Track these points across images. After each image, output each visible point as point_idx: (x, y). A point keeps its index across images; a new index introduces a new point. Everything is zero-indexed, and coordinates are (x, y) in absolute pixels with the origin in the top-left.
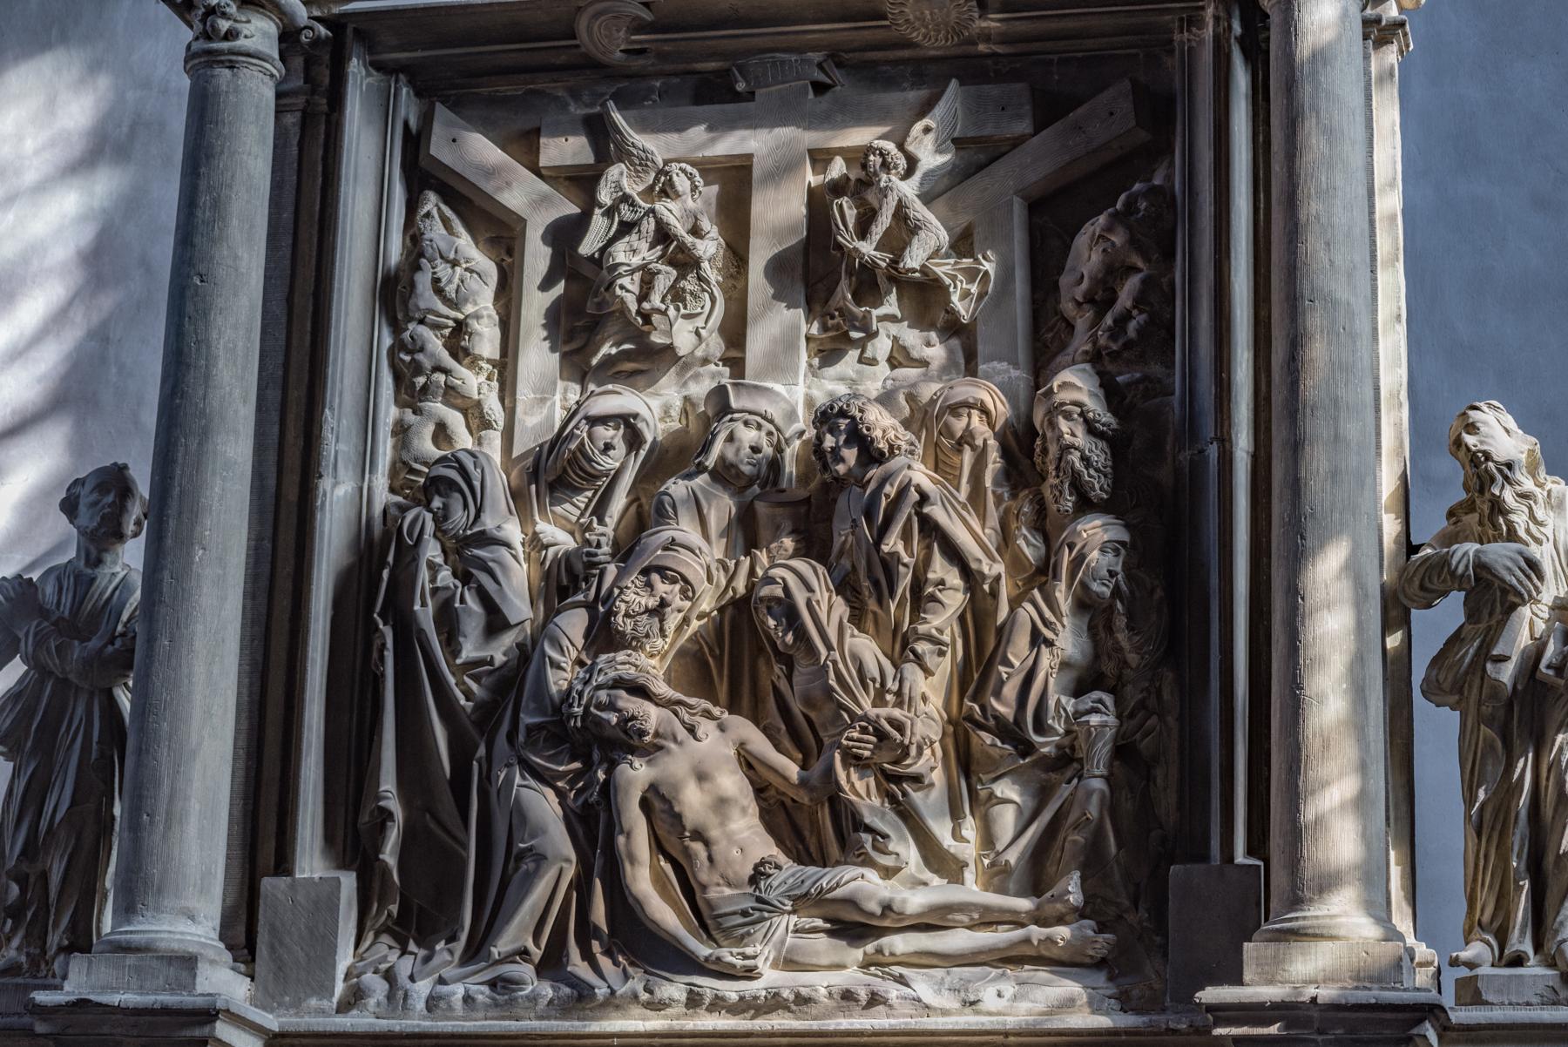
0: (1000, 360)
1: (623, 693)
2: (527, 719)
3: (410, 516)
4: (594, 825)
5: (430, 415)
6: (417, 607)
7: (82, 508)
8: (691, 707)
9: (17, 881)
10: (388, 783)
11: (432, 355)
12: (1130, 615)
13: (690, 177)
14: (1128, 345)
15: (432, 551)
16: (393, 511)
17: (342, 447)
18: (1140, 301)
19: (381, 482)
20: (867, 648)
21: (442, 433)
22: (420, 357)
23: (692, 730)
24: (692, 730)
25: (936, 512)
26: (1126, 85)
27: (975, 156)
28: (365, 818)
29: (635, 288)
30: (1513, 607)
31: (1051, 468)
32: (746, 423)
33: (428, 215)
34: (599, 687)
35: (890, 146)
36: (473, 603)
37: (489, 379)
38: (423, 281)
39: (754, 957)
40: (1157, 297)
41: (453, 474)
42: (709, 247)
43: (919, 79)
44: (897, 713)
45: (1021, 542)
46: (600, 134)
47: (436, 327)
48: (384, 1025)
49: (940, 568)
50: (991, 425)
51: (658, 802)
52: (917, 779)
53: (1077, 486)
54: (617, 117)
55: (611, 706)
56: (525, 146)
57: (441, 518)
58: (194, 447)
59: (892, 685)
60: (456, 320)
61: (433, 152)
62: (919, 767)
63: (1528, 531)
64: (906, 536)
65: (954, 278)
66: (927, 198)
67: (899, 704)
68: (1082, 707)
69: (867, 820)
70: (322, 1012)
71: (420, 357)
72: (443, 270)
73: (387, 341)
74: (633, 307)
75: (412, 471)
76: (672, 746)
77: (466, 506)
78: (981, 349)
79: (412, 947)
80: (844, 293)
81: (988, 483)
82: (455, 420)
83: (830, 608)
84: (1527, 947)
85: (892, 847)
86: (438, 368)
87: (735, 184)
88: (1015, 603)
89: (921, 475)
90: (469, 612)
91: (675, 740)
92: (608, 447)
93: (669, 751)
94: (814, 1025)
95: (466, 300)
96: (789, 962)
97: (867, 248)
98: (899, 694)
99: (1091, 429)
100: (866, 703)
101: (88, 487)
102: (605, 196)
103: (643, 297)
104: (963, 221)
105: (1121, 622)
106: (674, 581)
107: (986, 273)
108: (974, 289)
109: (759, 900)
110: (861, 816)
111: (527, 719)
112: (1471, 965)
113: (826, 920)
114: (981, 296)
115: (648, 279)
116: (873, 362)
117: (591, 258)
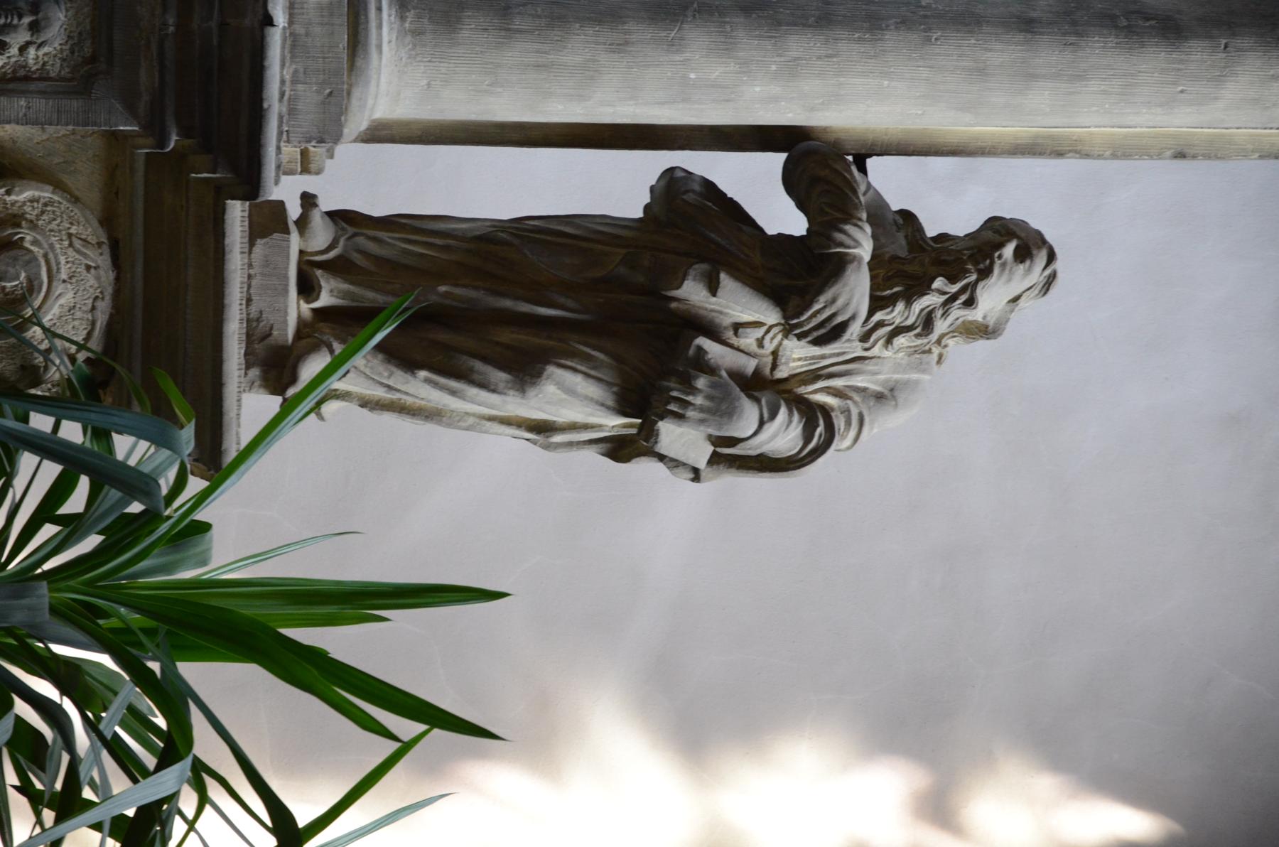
63: (880, 324)
84: (325, 300)
112: (302, 223)
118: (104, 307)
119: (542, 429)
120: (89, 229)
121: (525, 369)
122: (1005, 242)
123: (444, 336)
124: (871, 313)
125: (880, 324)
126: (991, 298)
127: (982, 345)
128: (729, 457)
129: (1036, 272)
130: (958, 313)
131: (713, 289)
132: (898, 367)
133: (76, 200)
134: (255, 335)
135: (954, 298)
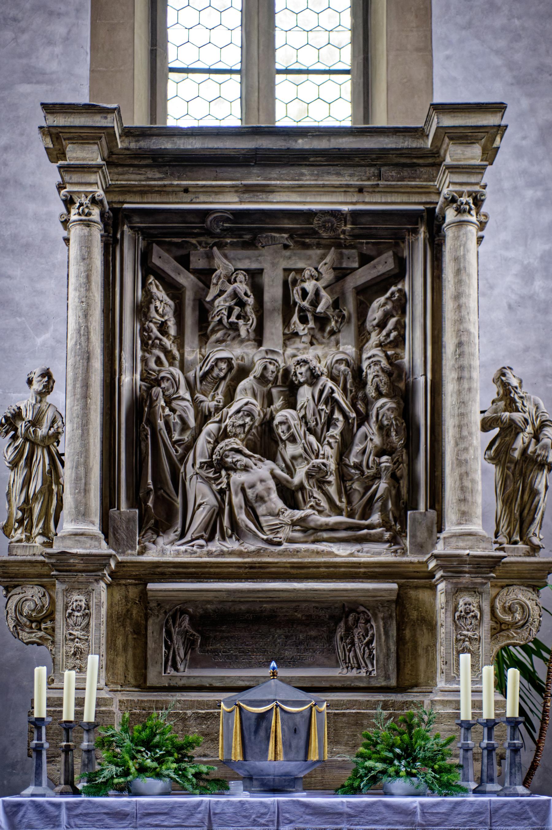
0: (348, 344)
1: (233, 452)
2: (199, 460)
3: (154, 389)
5: (154, 354)
6: (159, 421)
7: (34, 382)
8: (254, 457)
9: (21, 510)
10: (150, 481)
11: (155, 334)
12: (396, 432)
13: (245, 276)
14: (391, 342)
15: (163, 403)
16: (143, 387)
17: (127, 365)
18: (395, 329)
19: (138, 377)
20: (312, 438)
21: (159, 362)
22: (151, 334)
23: (256, 465)
25: (336, 395)
26: (391, 253)
27: (341, 274)
28: (142, 490)
29: (226, 313)
30: (517, 434)
31: (369, 383)
32: (270, 363)
33: (151, 283)
34: (226, 451)
36: (177, 420)
37: (173, 342)
38: (152, 307)
40: (400, 327)
42: (251, 300)
43: (318, 246)
44: (325, 461)
45: (359, 406)
46: (210, 257)
47: (155, 323)
48: (156, 559)
49: (337, 415)
50: (349, 366)
52: (329, 483)
56: (184, 262)
59: (322, 452)
61: (153, 261)
64: (326, 403)
65: (333, 317)
66: (325, 288)
67: (324, 458)
69: (315, 495)
70: (133, 555)
71: (151, 334)
72: (158, 304)
75: (149, 373)
77: (173, 387)
78: (341, 341)
79: (161, 534)
81: (348, 386)
83: (301, 426)
84: (518, 539)
85: (322, 504)
86: (157, 338)
87: (255, 277)
89: (330, 384)
91: (252, 468)
92: (221, 370)
94: (300, 560)
95: (165, 315)
96: (291, 541)
97: (306, 304)
98: (324, 455)
99: (383, 369)
100: (313, 457)
101: (37, 375)
102: (214, 281)
103: (229, 317)
105: (393, 434)
106: (248, 415)
107: (344, 315)
108: (340, 320)
109: (280, 520)
110: (312, 493)
111: (199, 460)
113: (301, 527)
115: (230, 310)
117: (208, 302)
118: (522, 588)
119: (547, 487)
120: (505, 591)
121: (534, 493)
122: (501, 379)
123: (526, 511)
124: (519, 411)
126: (515, 382)
127: (523, 383)
129: (508, 371)
130: (519, 390)
132: (530, 404)
133: (498, 594)
135: (515, 392)
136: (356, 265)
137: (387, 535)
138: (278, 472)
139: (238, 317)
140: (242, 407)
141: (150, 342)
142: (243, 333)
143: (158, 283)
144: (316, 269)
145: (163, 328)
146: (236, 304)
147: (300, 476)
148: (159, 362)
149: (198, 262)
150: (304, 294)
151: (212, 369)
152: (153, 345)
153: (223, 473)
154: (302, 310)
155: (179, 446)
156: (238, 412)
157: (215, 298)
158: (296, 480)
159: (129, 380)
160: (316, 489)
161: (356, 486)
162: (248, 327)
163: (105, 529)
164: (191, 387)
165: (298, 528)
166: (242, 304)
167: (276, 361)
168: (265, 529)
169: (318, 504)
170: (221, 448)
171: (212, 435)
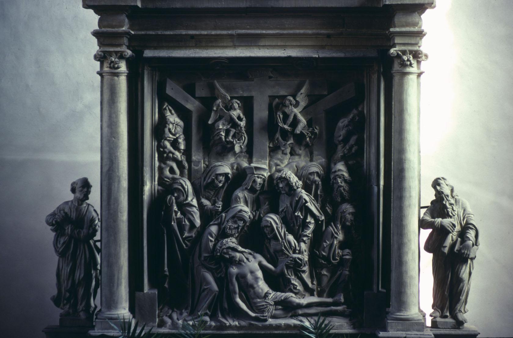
1: (230, 250)
4: (223, 281)
5: (168, 165)
10: (166, 269)
11: (169, 149)
13: (238, 104)
15: (175, 208)
20: (291, 237)
21: (172, 171)
22: (166, 150)
23: (247, 259)
24: (247, 259)
32: (258, 177)
34: (224, 249)
35: (291, 99)
38: (167, 130)
39: (266, 316)
40: (360, 143)
41: (180, 187)
42: (243, 124)
44: (300, 256)
45: (327, 208)
47: (169, 141)
49: (309, 219)
51: (241, 277)
52: (304, 272)
53: (341, 194)
54: (217, 85)
55: (227, 253)
56: (190, 90)
57: (177, 198)
58: (116, 185)
59: (298, 248)
60: (174, 139)
62: (304, 269)
67: (299, 253)
68: (344, 254)
72: (171, 126)
73: (156, 144)
74: (224, 140)
76: (243, 264)
79: (175, 310)
80: (278, 135)
81: (319, 193)
82: (174, 166)
86: (170, 152)
88: (326, 227)
90: (186, 224)
91: (244, 262)
92: (220, 182)
93: (243, 265)
96: (274, 317)
97: (286, 127)
99: (345, 181)
100: (291, 252)
102: (215, 109)
104: (309, 117)
106: (241, 220)
109: (266, 302)
114: (314, 138)
116: (286, 154)
125: (452, 213)
126: (447, 191)
127: (455, 189)
128: (476, 244)
129: (442, 182)
131: (446, 247)
134: (454, 327)
136: (326, 93)
137: (348, 311)
138: (265, 263)
139: (234, 136)
140: (236, 214)
141: (165, 155)
142: (237, 149)
143: (170, 108)
144: (295, 99)
145: (175, 144)
146: (231, 127)
147: (282, 266)
148: (172, 171)
149: (201, 92)
150: (286, 117)
151: (213, 180)
152: (168, 158)
153: (222, 264)
154: (283, 130)
155: (188, 241)
156: (233, 217)
157: (216, 121)
158: (279, 269)
159: (148, 188)
160: (293, 277)
161: (324, 272)
162: (241, 144)
163: (132, 309)
164: (197, 194)
165: (280, 307)
166: (235, 125)
167: (263, 175)
168: (254, 308)
169: (296, 289)
170: (221, 247)
171: (214, 235)
